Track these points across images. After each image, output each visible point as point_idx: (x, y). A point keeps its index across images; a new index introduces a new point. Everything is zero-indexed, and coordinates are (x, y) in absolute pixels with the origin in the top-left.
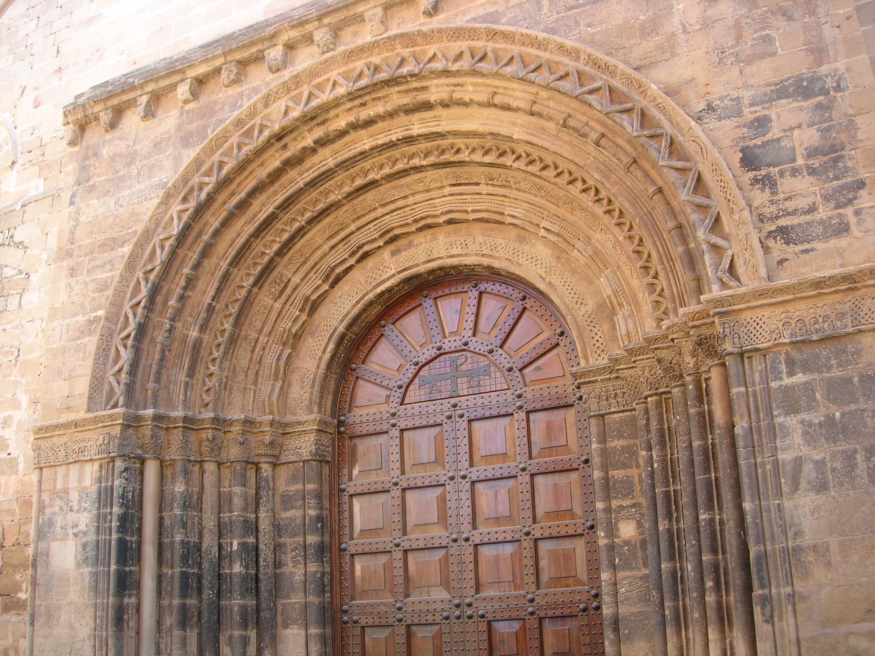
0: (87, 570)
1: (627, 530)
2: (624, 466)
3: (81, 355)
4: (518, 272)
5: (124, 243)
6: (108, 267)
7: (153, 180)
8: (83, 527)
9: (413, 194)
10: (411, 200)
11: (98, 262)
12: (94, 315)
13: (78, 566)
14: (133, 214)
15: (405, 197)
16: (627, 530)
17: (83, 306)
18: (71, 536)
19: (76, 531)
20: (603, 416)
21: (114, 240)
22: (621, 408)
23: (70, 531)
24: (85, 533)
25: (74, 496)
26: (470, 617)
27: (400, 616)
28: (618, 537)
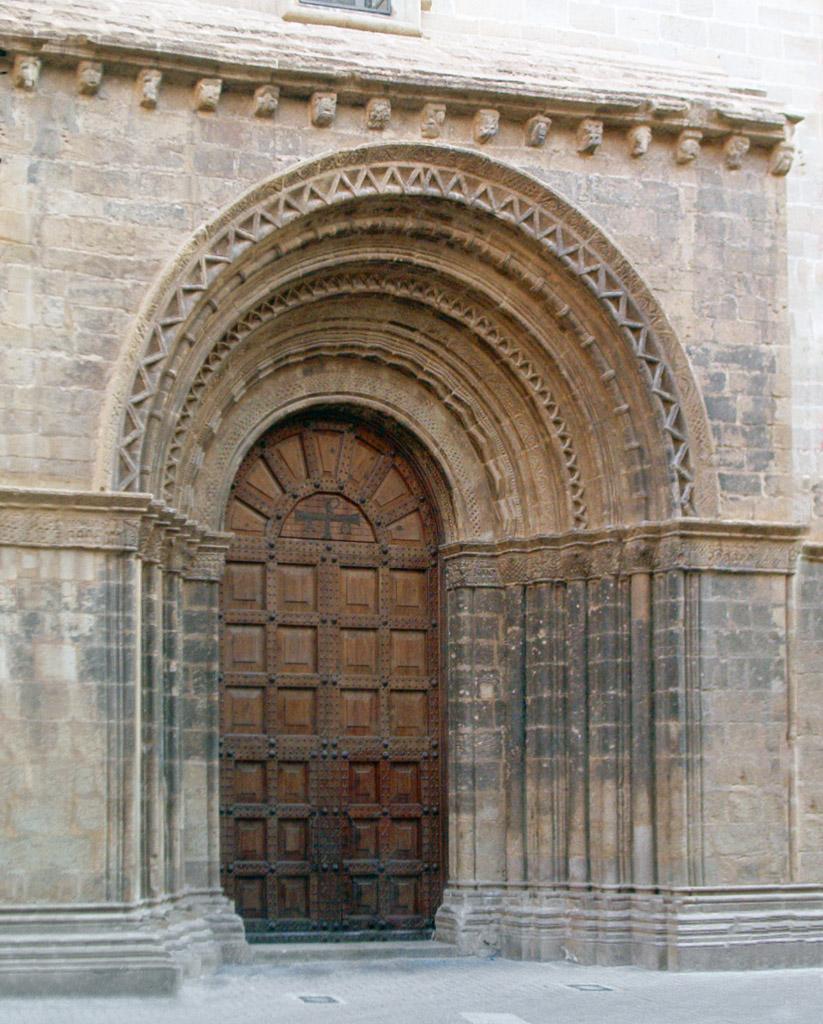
0: (93, 684)
1: (487, 692)
2: (488, 636)
3: (68, 409)
4: (417, 431)
5: (125, 272)
6: (103, 298)
7: (162, 199)
8: (86, 631)
9: (354, 319)
10: (349, 324)
11: (85, 286)
12: (85, 357)
13: (82, 676)
14: (132, 236)
15: (346, 319)
16: (487, 692)
17: (66, 339)
18: (68, 641)
19: (75, 634)
20: (473, 589)
21: (110, 263)
22: (490, 584)
23: (67, 634)
24: (89, 639)
25: (69, 593)
26: (335, 758)
27: (272, 752)
28: (478, 697)
